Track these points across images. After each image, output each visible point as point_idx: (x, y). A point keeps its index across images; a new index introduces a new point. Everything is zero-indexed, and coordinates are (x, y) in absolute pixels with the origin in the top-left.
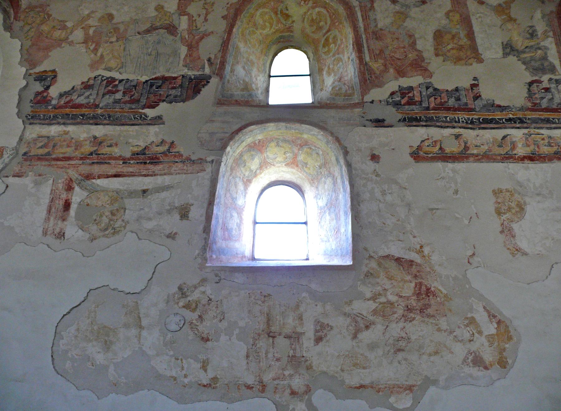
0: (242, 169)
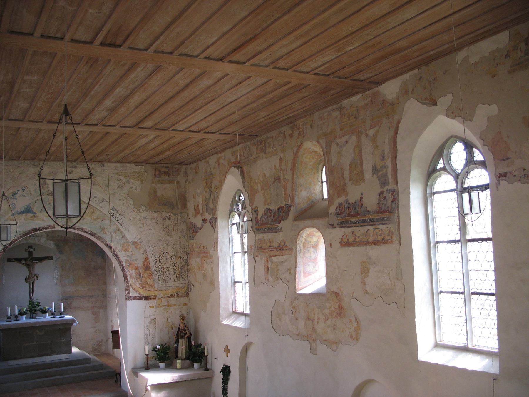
0: (310, 243)
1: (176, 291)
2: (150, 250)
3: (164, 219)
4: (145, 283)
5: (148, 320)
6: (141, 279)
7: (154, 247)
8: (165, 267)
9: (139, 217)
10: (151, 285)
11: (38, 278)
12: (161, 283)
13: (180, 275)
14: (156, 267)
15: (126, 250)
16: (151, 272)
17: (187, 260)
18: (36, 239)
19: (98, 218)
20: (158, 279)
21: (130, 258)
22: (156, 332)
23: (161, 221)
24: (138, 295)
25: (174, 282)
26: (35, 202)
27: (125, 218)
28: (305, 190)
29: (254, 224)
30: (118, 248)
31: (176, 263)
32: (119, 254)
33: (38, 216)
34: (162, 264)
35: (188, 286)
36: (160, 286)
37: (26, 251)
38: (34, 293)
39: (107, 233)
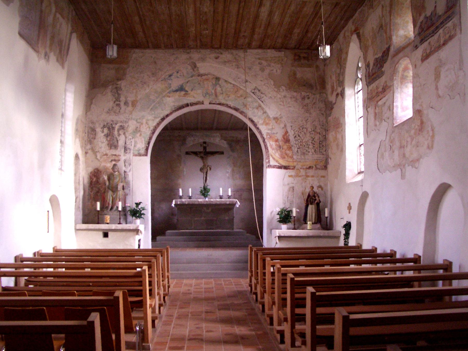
1: (314, 163)
3: (303, 98)
4: (284, 154)
5: (287, 188)
8: (304, 141)
9: (279, 96)
11: (210, 169)
14: (295, 140)
15: (267, 124)
17: (325, 136)
18: (212, 139)
19: (241, 96)
20: (297, 151)
22: (294, 199)
24: (278, 165)
26: (187, 82)
28: (403, 29)
29: (367, 78)
32: (261, 127)
33: (189, 94)
35: (326, 159)
37: (201, 145)
38: (207, 181)
39: (250, 109)
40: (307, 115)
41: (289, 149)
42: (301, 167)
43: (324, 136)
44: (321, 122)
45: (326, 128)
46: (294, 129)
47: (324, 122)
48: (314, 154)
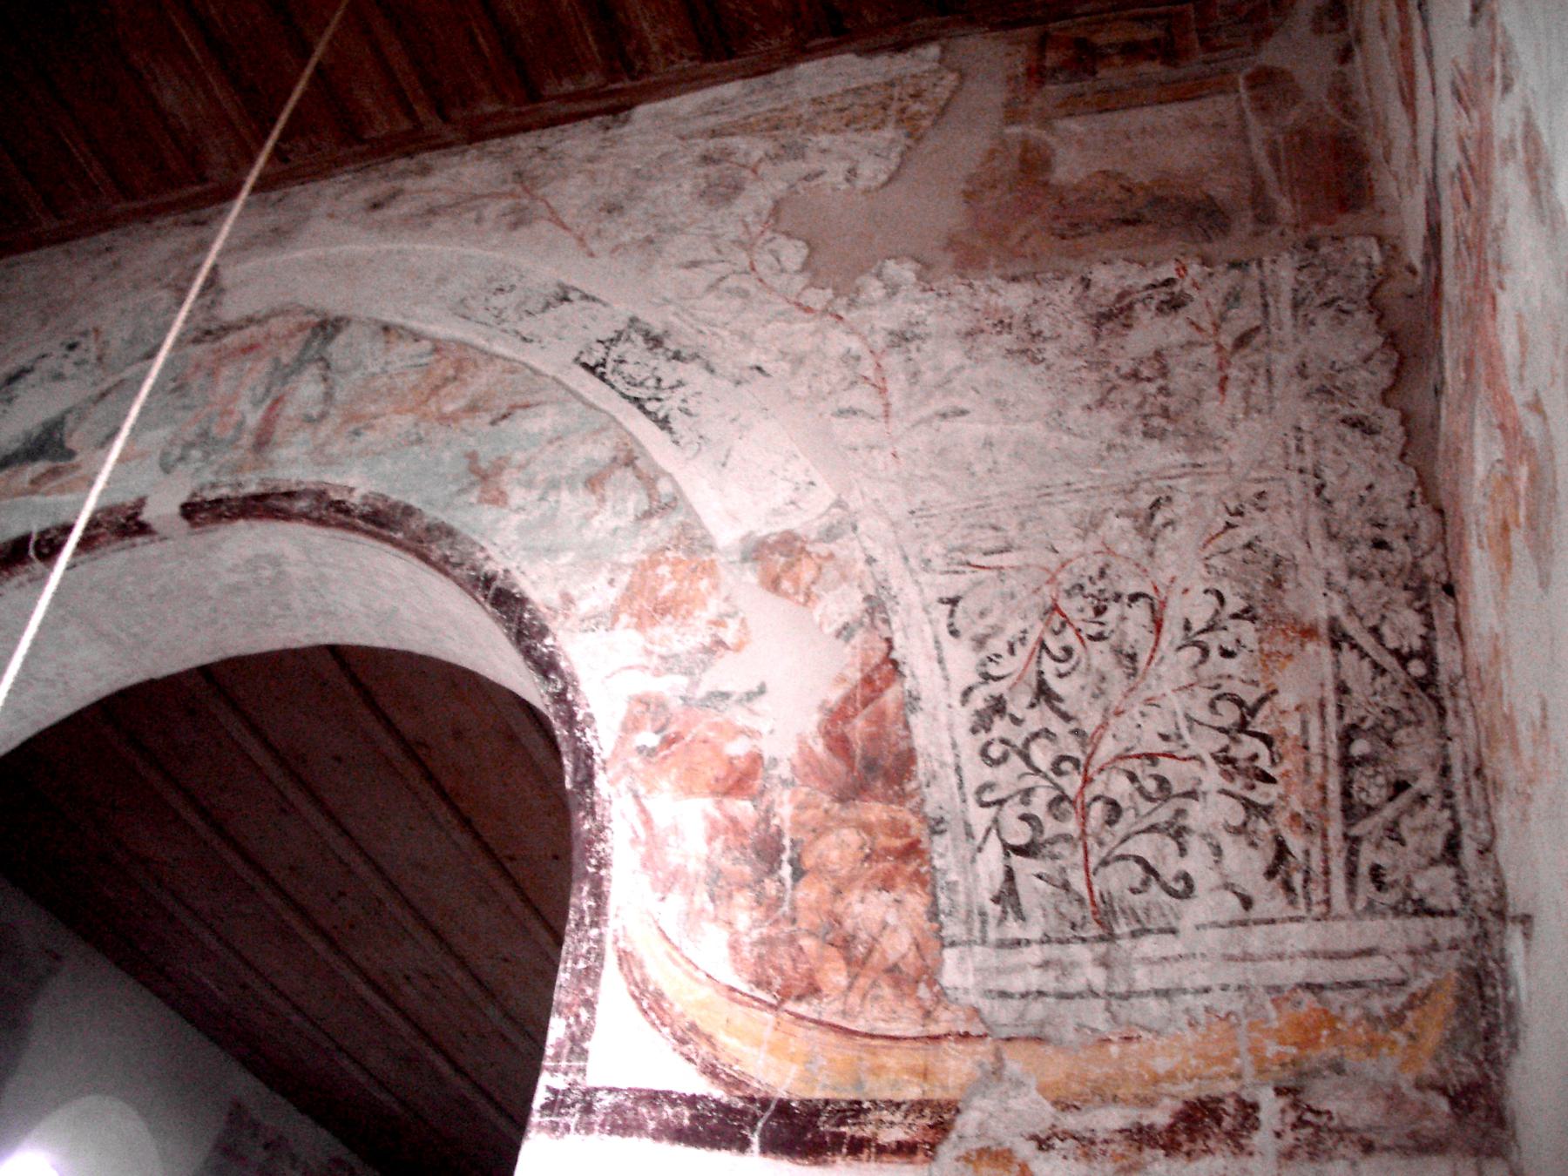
1: (1271, 1049)
2: (932, 595)
4: (807, 943)
6: (771, 887)
7: (984, 561)
8: (1107, 749)
9: (840, 341)
10: (893, 970)
12: (1046, 940)
13: (1336, 842)
14: (984, 753)
16: (918, 811)
20: (1008, 895)
21: (682, 681)
23: (1079, 333)
24: (695, 1083)
25: (1244, 924)
27: (712, 371)
30: (584, 595)
31: (1262, 700)
34: (1066, 717)
36: (1017, 984)
39: (517, 496)
40: (1158, 457)
41: (887, 865)
42: (1043, 1115)
43: (1403, 658)
44: (1341, 506)
45: (1430, 565)
46: (980, 629)
47: (1395, 510)
48: (1261, 909)
